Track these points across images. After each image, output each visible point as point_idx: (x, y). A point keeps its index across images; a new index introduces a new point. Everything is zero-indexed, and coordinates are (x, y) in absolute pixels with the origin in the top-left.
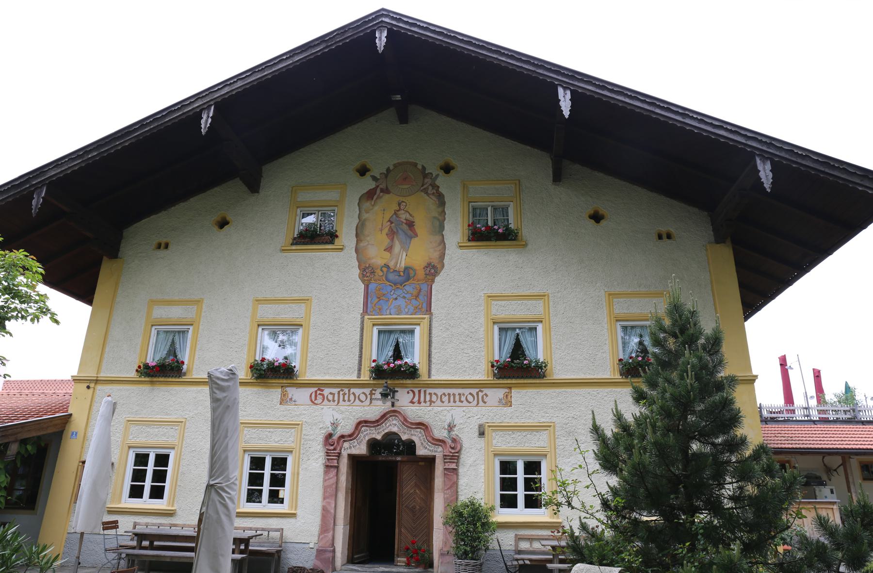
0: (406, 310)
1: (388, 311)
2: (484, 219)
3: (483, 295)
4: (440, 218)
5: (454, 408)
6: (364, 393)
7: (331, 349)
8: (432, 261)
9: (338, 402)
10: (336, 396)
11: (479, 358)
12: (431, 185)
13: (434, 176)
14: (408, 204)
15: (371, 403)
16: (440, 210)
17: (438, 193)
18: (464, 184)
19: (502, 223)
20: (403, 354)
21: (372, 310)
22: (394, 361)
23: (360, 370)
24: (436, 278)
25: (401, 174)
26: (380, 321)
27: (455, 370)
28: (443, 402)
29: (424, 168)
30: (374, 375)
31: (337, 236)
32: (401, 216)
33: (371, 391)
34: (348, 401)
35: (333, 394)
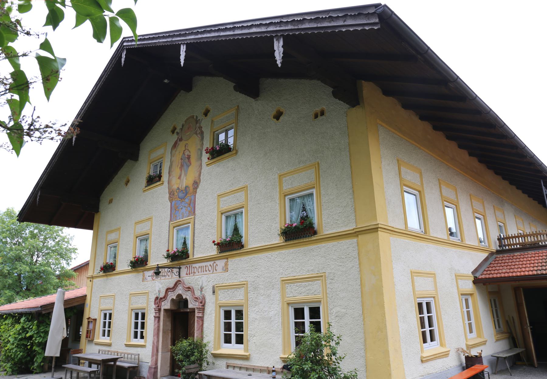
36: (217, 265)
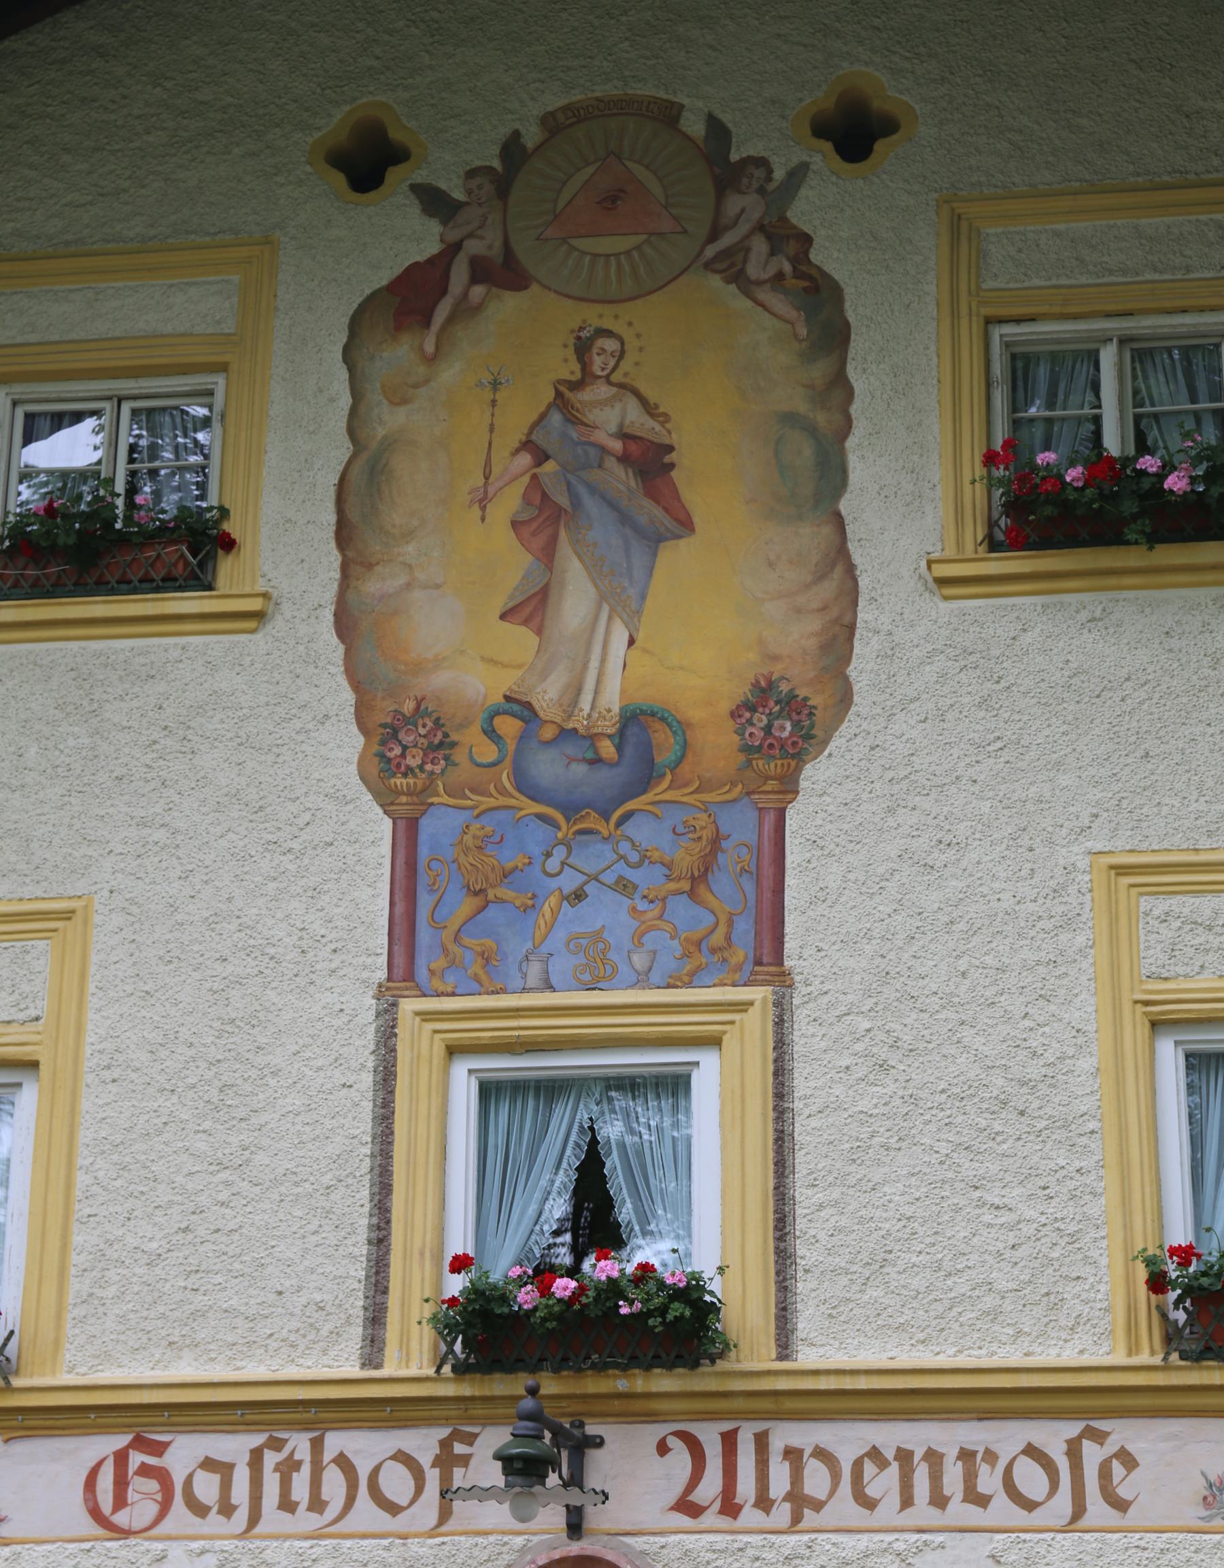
0: (639, 960)
1: (534, 971)
2: (1079, 420)
3: (1083, 863)
4: (821, 419)
5: (939, 1538)
6: (402, 1457)
7: (203, 1199)
8: (778, 670)
9: (254, 1518)
10: (241, 1477)
11: (1074, 1238)
12: (760, 228)
13: (779, 174)
14: (632, 344)
15: (445, 1514)
16: (819, 371)
17: (810, 278)
18: (956, 221)
19: (1186, 435)
20: (625, 1212)
21: (439, 963)
22: (579, 1254)
23: (376, 1318)
24: (808, 770)
25: (590, 170)
26: (486, 1030)
27: (939, 1307)
28: (870, 1504)
29: (718, 132)
30: (458, 1347)
31: (228, 544)
32: (594, 416)
33: (445, 1444)
34: (310, 1509)
35: (223, 1469)
36: (1128, 1459)
